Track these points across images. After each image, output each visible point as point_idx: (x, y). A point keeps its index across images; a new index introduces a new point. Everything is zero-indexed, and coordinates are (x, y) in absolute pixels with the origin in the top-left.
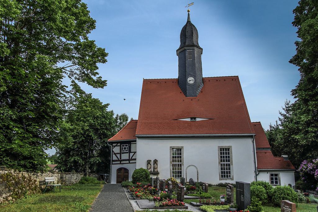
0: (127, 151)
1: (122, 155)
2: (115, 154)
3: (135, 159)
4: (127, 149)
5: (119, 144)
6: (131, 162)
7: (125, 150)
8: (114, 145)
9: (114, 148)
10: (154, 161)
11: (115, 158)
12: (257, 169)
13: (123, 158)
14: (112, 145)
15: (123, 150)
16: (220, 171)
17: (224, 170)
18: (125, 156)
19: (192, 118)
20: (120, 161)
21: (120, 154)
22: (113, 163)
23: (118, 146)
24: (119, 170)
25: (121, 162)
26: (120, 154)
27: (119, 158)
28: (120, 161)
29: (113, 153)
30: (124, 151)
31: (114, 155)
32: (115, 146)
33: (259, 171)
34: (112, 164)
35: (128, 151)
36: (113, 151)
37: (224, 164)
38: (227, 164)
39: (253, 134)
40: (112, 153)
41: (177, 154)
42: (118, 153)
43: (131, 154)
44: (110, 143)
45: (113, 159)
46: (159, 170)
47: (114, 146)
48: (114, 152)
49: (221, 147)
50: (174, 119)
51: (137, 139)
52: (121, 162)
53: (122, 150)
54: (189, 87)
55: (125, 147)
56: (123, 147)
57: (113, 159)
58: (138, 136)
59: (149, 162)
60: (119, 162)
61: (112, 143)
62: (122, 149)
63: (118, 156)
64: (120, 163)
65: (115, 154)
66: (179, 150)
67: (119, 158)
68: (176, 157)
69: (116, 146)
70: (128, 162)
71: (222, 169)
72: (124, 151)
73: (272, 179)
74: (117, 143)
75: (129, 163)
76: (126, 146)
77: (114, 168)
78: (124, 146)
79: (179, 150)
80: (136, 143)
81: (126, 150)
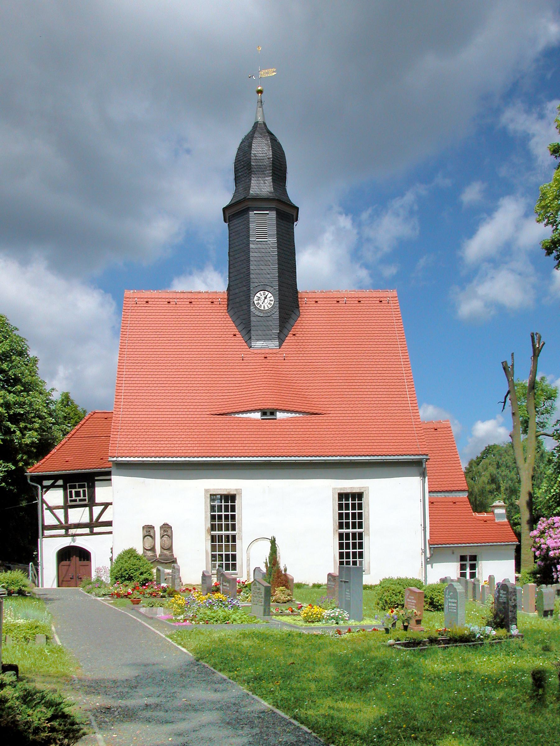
0: (85, 500)
1: (70, 511)
2: (50, 509)
3: (109, 524)
4: (84, 496)
5: (60, 482)
6: (96, 530)
7: (78, 498)
8: (46, 483)
9: (46, 491)
10: (161, 528)
11: (49, 519)
12: (430, 544)
13: (72, 521)
14: (41, 485)
15: (74, 498)
16: (337, 551)
17: (348, 547)
18: (79, 515)
19: (264, 413)
20: (67, 527)
21: (66, 507)
22: (47, 533)
24: (65, 555)
25: (67, 531)
26: (66, 507)
27: (63, 521)
28: (67, 527)
30: (76, 501)
31: (47, 513)
32: (48, 488)
33: (436, 550)
35: (87, 502)
36: (43, 501)
37: (347, 535)
38: (354, 534)
39: (421, 457)
41: (224, 511)
42: (58, 507)
43: (97, 510)
44: (34, 478)
45: (46, 524)
46: (177, 552)
47: (45, 487)
49: (341, 489)
50: (216, 412)
51: (113, 470)
52: (67, 531)
53: (69, 499)
54: (258, 319)
56: (73, 491)
57: (46, 524)
58: (115, 459)
59: (148, 531)
60: (63, 532)
61: (39, 479)
62: (71, 497)
63: (60, 513)
64: (67, 535)
65: (50, 509)
66: (230, 498)
67: (63, 521)
68: (220, 517)
69: (53, 486)
70: (87, 530)
71: (341, 546)
72: (76, 501)
73: (463, 567)
74: (55, 478)
75: (92, 533)
76: (81, 486)
77: (49, 548)
78: (74, 487)
79: (230, 498)
80: (110, 480)
81: (82, 497)
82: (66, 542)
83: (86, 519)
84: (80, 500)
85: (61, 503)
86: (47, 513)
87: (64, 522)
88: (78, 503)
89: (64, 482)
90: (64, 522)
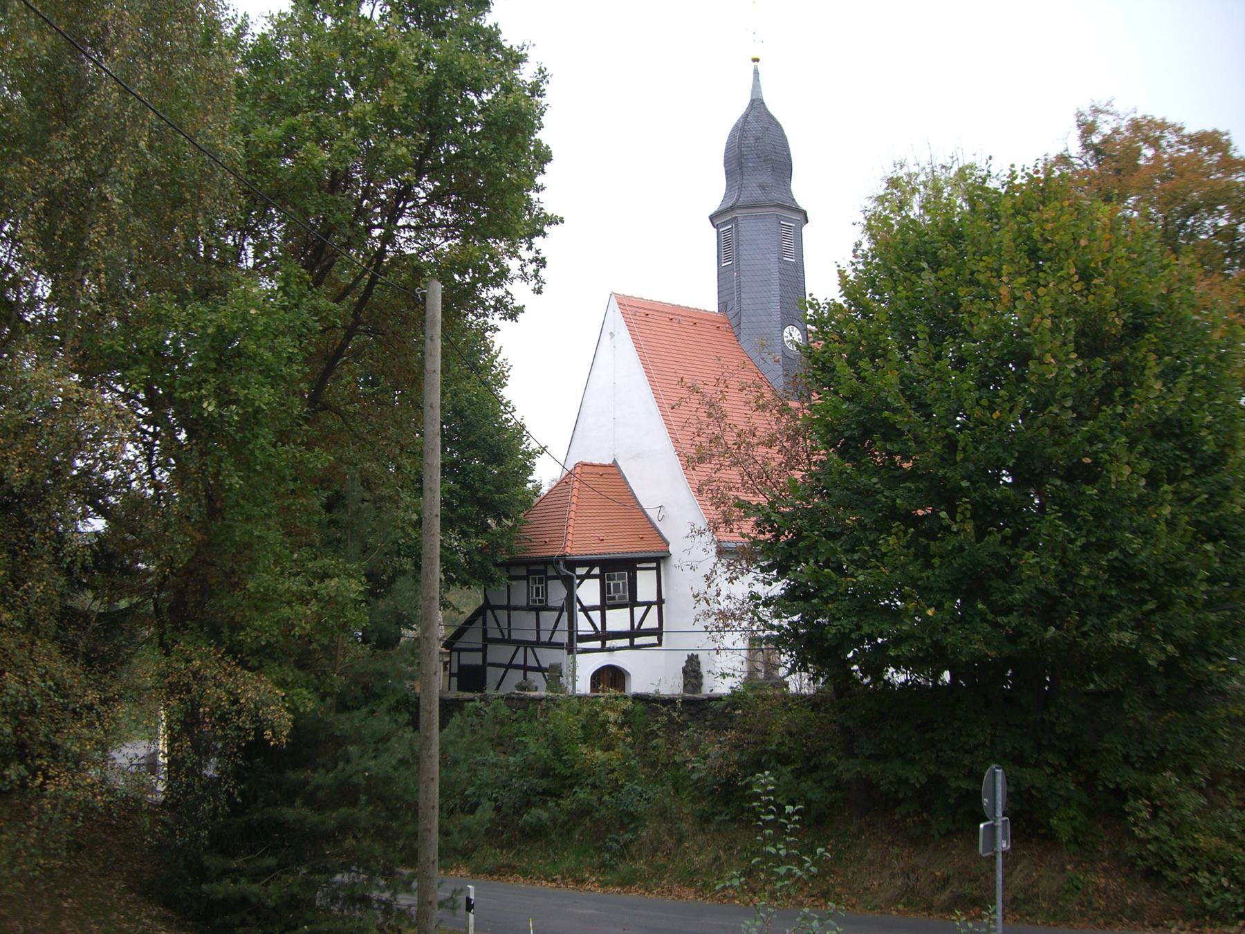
2: (585, 610)
5: (596, 571)
6: (638, 641)
8: (581, 571)
11: (583, 626)
18: (618, 620)
21: (603, 608)
23: (594, 577)
25: (604, 644)
26: (603, 608)
31: (581, 616)
32: (582, 578)
42: (594, 608)
43: (639, 611)
47: (579, 577)
52: (604, 644)
60: (598, 644)
63: (596, 615)
64: (603, 649)
65: (585, 610)
69: (588, 576)
70: (626, 642)
74: (590, 563)
75: (632, 646)
82: (602, 660)
83: (626, 627)
85: (598, 603)
86: (581, 616)
88: (617, 601)
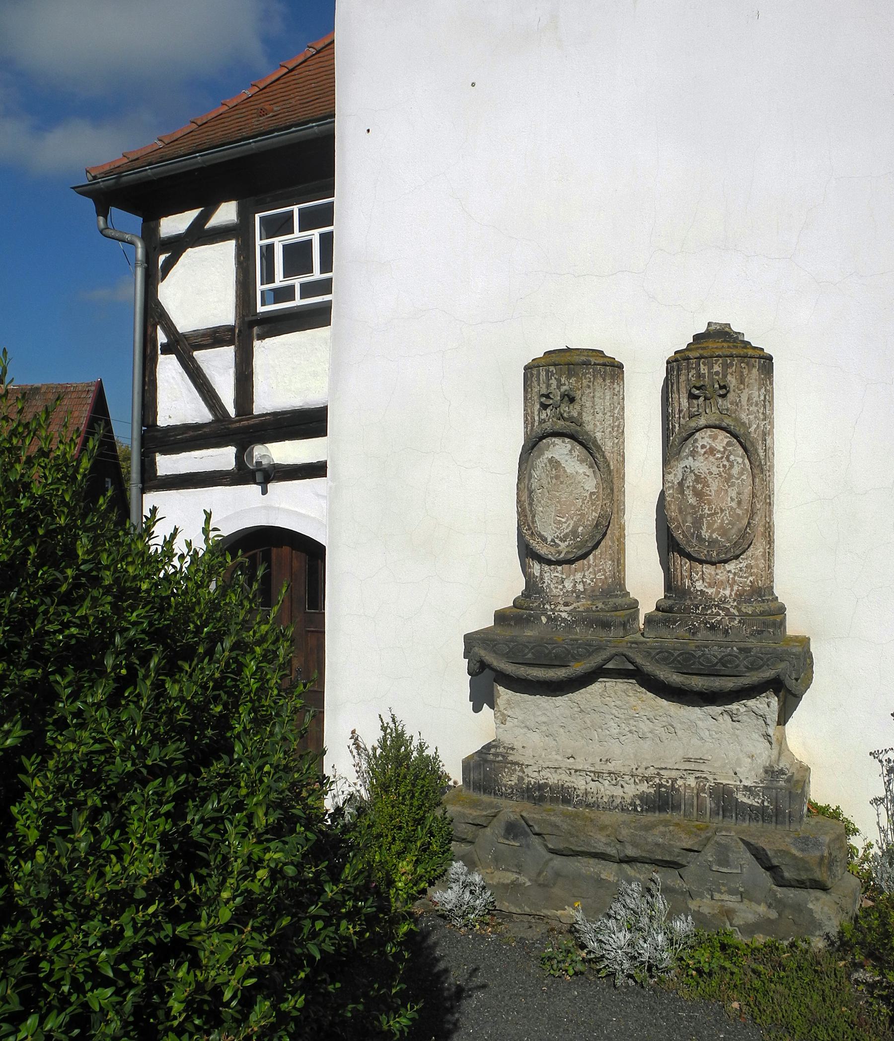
1: (268, 352)
5: (226, 213)
7: (297, 282)
13: (268, 398)
15: (280, 280)
21: (246, 331)
22: (167, 464)
26: (246, 331)
29: (162, 338)
31: (168, 368)
32: (177, 246)
34: (152, 481)
40: (148, 340)
42: (215, 337)
45: (163, 420)
48: (170, 328)
53: (260, 288)
55: (297, 236)
56: (279, 243)
57: (163, 420)
60: (223, 458)
62: (269, 277)
63: (219, 364)
64: (243, 474)
65: (184, 347)
69: (199, 235)
72: (286, 294)
78: (281, 226)
84: (308, 290)
85: (222, 311)
86: (168, 368)
87: (232, 412)
88: (298, 301)
89: (241, 213)
90: (232, 412)
